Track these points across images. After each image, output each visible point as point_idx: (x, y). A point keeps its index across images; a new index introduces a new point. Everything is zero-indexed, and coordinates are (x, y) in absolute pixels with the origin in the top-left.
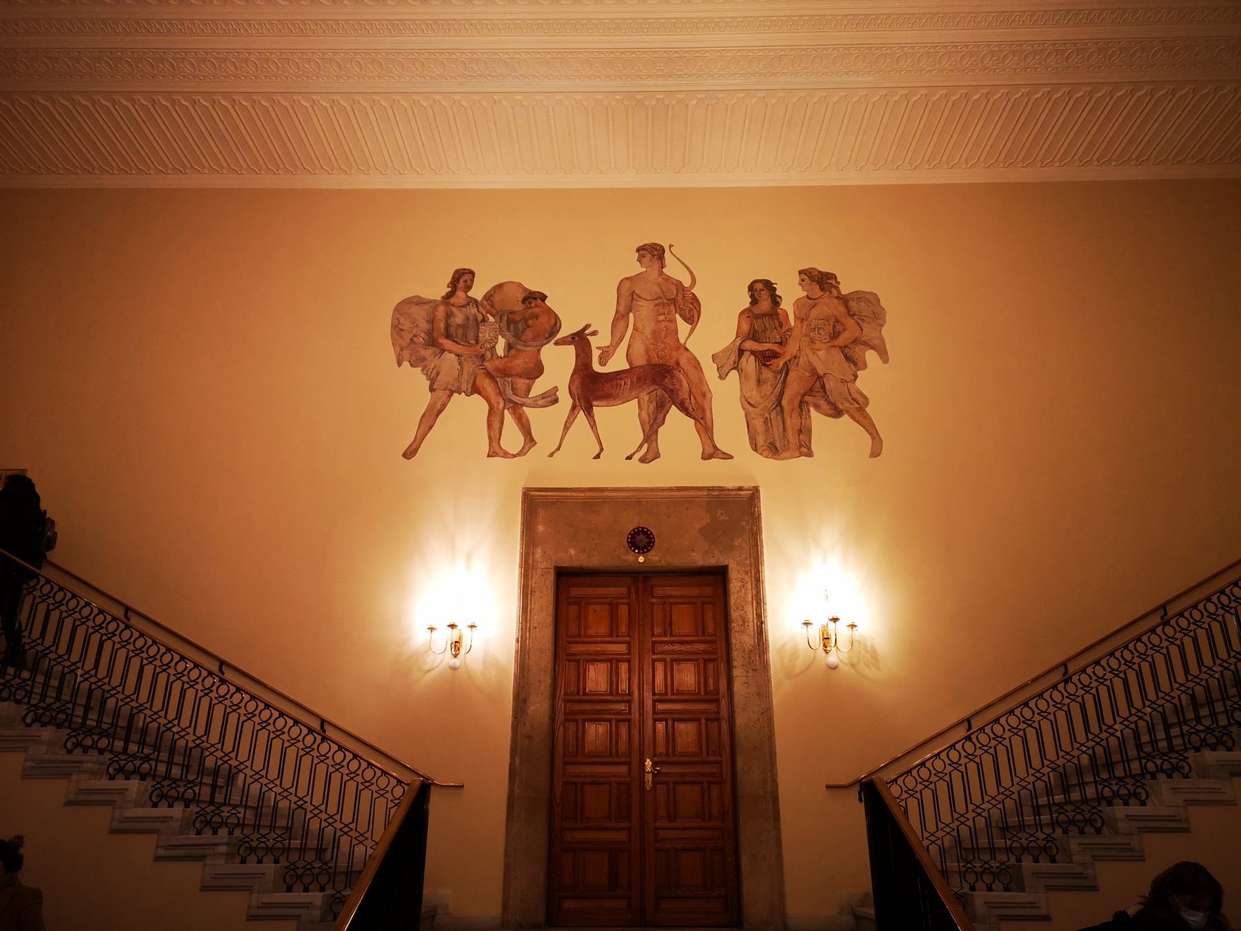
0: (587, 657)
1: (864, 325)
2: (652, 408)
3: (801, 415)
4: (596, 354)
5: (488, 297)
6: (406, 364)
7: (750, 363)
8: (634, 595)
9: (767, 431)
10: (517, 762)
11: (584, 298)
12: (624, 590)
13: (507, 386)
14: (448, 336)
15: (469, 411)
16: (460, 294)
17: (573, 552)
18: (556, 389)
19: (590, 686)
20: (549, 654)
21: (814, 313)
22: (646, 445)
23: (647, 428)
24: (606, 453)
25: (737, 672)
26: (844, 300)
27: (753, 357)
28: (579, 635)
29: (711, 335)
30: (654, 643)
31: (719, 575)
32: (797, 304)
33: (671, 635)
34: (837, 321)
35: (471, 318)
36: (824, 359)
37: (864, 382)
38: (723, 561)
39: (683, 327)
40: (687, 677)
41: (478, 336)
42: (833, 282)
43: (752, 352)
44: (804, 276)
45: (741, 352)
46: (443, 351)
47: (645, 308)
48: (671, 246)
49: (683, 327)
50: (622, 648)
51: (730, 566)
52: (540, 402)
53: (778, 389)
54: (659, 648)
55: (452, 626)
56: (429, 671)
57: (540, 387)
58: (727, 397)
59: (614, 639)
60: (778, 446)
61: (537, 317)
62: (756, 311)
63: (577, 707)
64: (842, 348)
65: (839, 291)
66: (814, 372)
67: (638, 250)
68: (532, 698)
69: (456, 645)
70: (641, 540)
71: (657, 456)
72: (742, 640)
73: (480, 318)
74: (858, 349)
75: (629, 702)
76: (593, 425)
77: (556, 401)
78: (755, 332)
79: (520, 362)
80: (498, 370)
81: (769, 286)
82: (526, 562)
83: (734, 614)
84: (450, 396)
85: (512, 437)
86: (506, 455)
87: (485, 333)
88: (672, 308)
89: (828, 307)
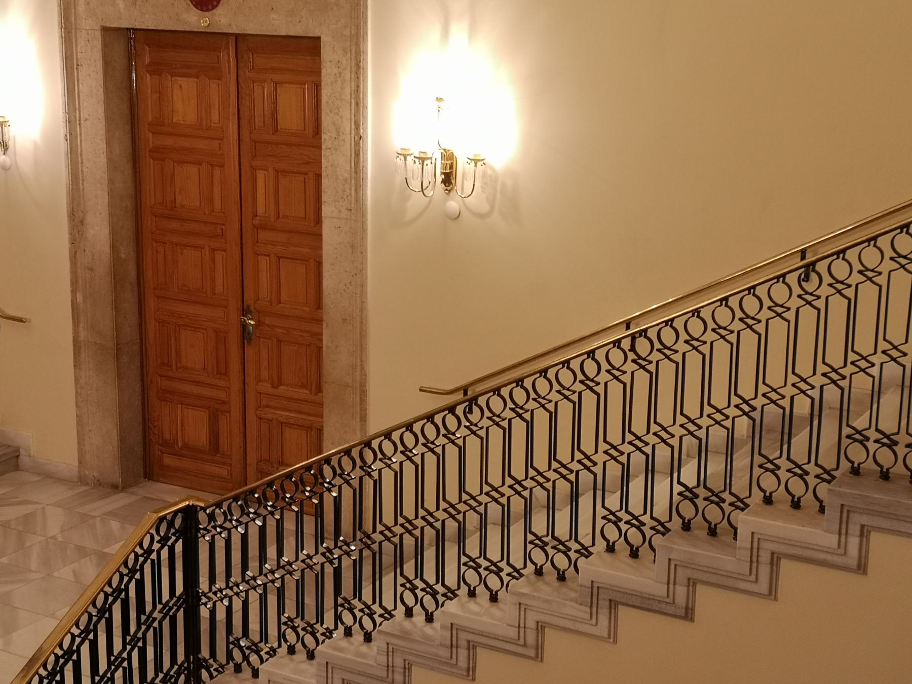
10: (80, 298)
51: (324, 39)
68: (90, 219)
72: (333, 161)
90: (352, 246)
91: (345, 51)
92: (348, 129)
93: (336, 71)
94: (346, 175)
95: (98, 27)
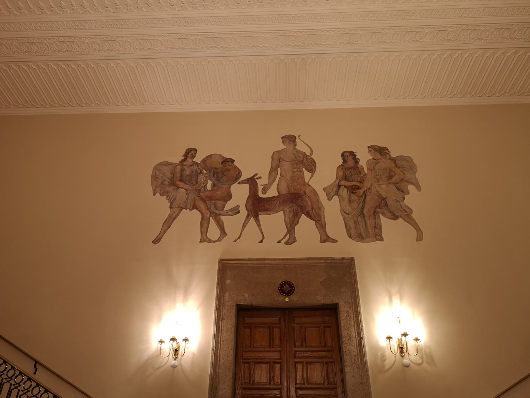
0: (255, 360)
1: (406, 172)
2: (291, 216)
3: (375, 219)
4: (260, 188)
5: (204, 161)
6: (158, 195)
7: (344, 192)
8: (283, 322)
9: (356, 227)
11: (254, 161)
12: (276, 319)
13: (212, 205)
14: (181, 180)
15: (191, 218)
16: (189, 160)
17: (247, 295)
18: (238, 206)
19: (257, 379)
20: (231, 358)
21: (377, 167)
22: (288, 235)
23: (289, 226)
24: (266, 240)
25: (347, 369)
26: (394, 160)
27: (345, 189)
28: (250, 347)
29: (324, 177)
30: (296, 351)
31: (332, 310)
32: (368, 162)
33: (306, 347)
34: (390, 170)
35: (194, 171)
36: (385, 189)
37: (408, 201)
38: (335, 301)
39: (307, 175)
40: (317, 374)
41: (197, 180)
42: (387, 151)
43: (345, 186)
44: (370, 149)
45: (339, 186)
46: (178, 188)
47: (286, 165)
48: (299, 136)
49: (307, 175)
50: (277, 355)
51: (341, 304)
52: (230, 213)
53: (361, 205)
54: (299, 355)
55: (173, 339)
56: (159, 368)
57: (229, 205)
58: (333, 210)
59: (272, 349)
60: (363, 235)
61: (229, 171)
62: (346, 166)
63: (248, 392)
64: (395, 184)
65: (390, 156)
66: (380, 196)
67: (282, 138)
69: (176, 351)
70: (286, 288)
71: (295, 241)
72: (349, 348)
73: (199, 171)
74: (403, 184)
75: (281, 389)
76: (259, 225)
77: (238, 212)
78: (346, 176)
79: (219, 193)
80: (207, 197)
81: (352, 154)
82: (220, 301)
83: (344, 333)
84: (180, 211)
85: (213, 231)
86: (210, 241)
87: (201, 179)
88: (301, 165)
89: (384, 163)
90: (361, 383)
91: (350, 307)
92: (354, 336)
93: (346, 314)
94: (355, 354)
95: (235, 304)
